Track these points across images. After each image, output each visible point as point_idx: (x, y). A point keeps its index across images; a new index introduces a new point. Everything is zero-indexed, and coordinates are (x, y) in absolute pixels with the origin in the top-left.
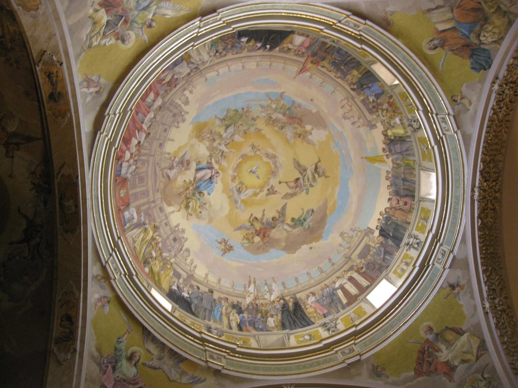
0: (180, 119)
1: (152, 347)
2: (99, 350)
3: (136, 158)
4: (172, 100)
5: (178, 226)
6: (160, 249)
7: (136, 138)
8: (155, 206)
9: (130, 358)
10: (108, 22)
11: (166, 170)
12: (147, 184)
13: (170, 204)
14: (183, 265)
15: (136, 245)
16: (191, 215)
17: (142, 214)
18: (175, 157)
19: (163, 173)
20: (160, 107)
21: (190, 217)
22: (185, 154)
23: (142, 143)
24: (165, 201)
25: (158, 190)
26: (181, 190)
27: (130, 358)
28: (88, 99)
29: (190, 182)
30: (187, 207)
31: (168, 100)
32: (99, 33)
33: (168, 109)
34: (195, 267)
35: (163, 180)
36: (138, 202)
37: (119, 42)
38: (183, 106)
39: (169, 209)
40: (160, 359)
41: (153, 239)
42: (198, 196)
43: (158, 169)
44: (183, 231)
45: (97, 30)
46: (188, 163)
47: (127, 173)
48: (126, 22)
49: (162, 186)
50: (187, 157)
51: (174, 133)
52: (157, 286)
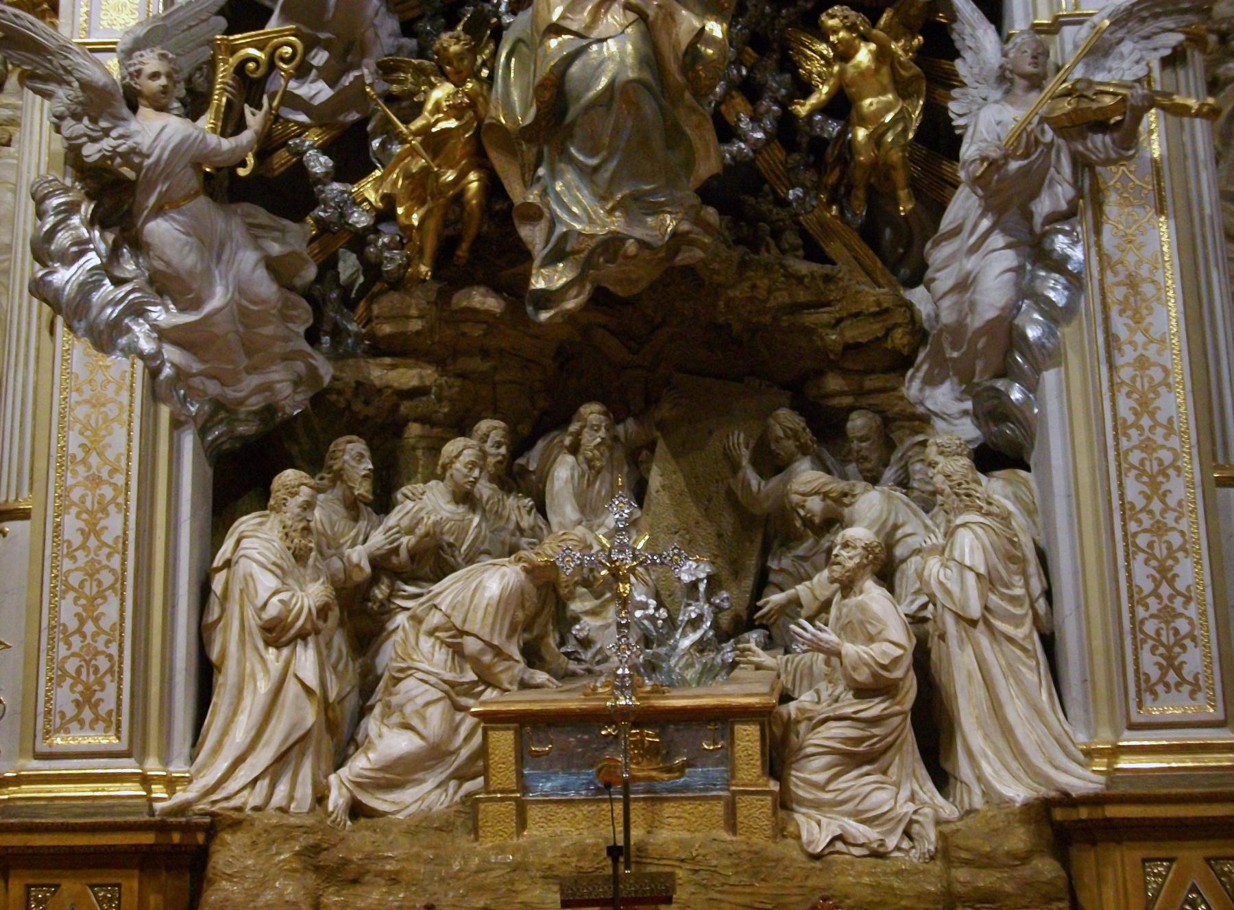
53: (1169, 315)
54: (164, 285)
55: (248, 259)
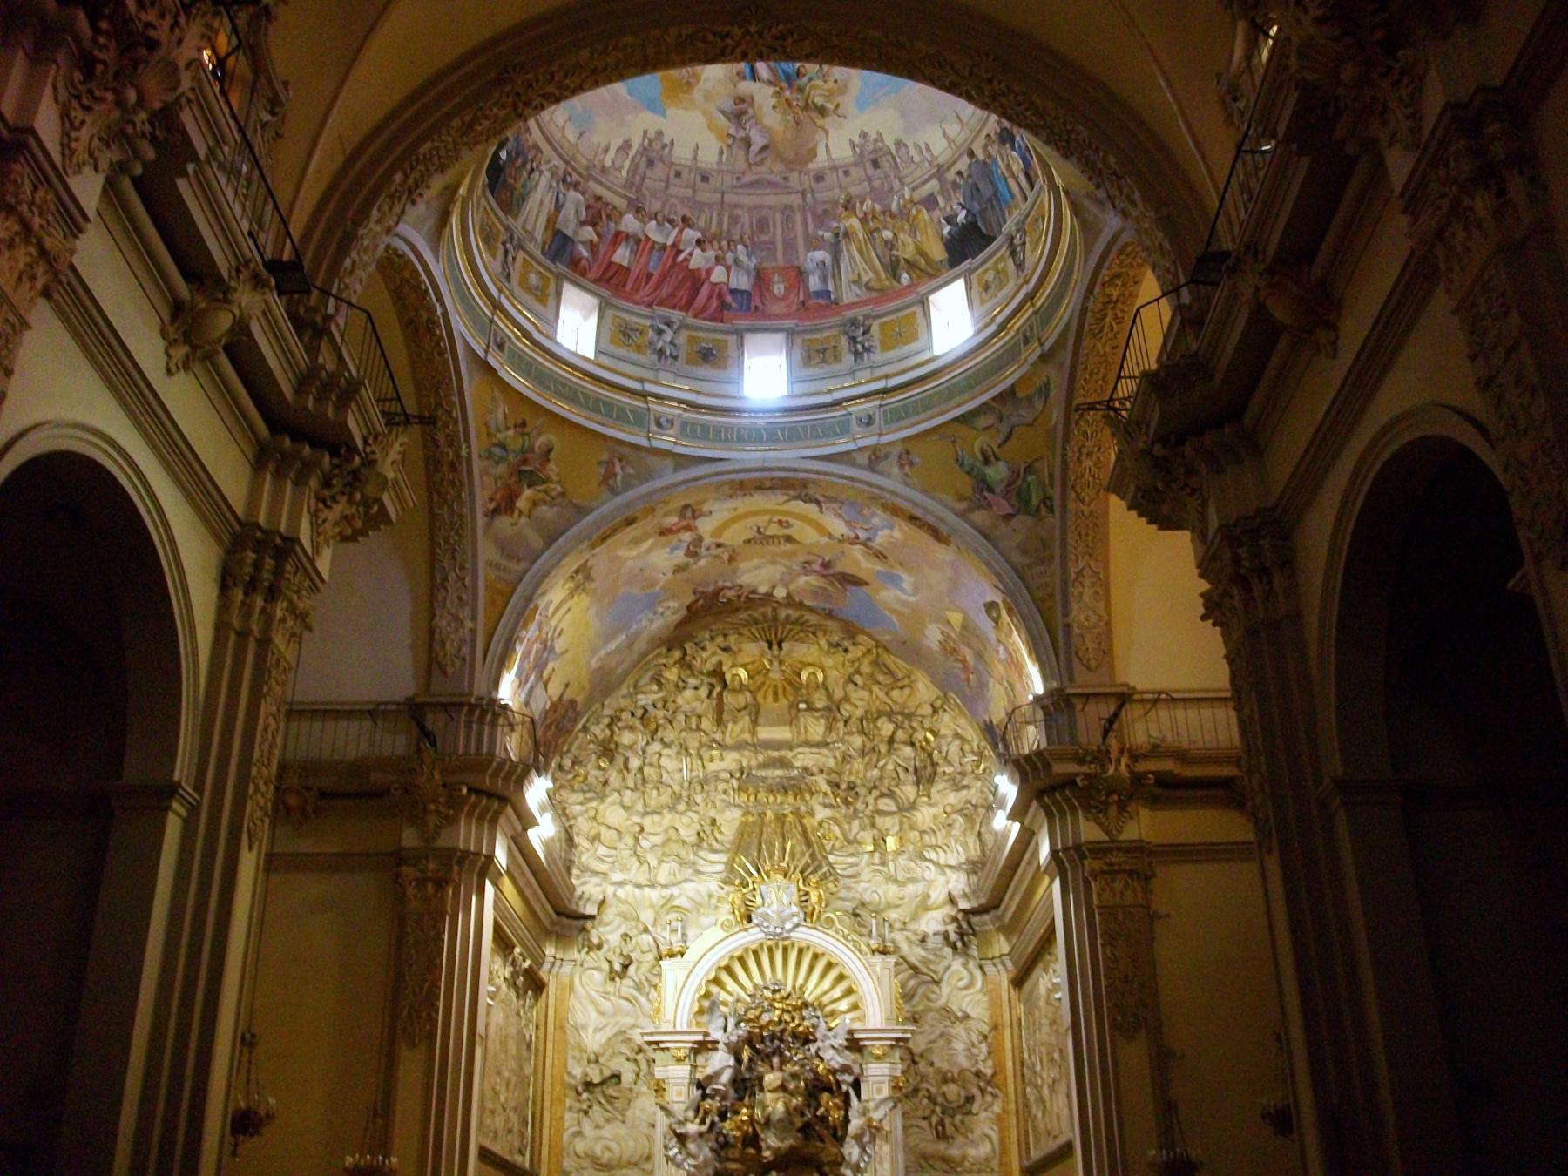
0: (657, 146)
1: (982, 422)
2: (961, 498)
3: (724, 243)
4: (624, 186)
5: (853, 146)
6: (884, 213)
7: (691, 254)
8: (812, 192)
9: (987, 462)
10: (529, 486)
11: (751, 155)
12: (770, 207)
13: (813, 153)
14: (918, 173)
15: (865, 279)
16: (838, 106)
17: (821, 233)
18: (729, 135)
19: (757, 164)
20: (638, 211)
21: (840, 111)
22: (723, 112)
23: (699, 235)
24: (806, 162)
25: (785, 179)
26: (790, 118)
27: (987, 462)
28: (631, 471)
29: (777, 94)
30: (822, 111)
31: (625, 197)
32: (545, 491)
33: (639, 190)
34: (928, 148)
35: (768, 162)
36: (800, 240)
37: (552, 456)
38: (632, 153)
39: (821, 160)
40: (1001, 420)
41: (864, 221)
42: (805, 80)
43: (748, 178)
44: (864, 135)
45: (541, 495)
46: (740, 100)
47: (748, 271)
48: (525, 462)
49: (779, 167)
50: (729, 105)
51: (682, 153)
52: (932, 276)
53: (887, 1165)
54: (689, 1155)
55: (707, 1151)
